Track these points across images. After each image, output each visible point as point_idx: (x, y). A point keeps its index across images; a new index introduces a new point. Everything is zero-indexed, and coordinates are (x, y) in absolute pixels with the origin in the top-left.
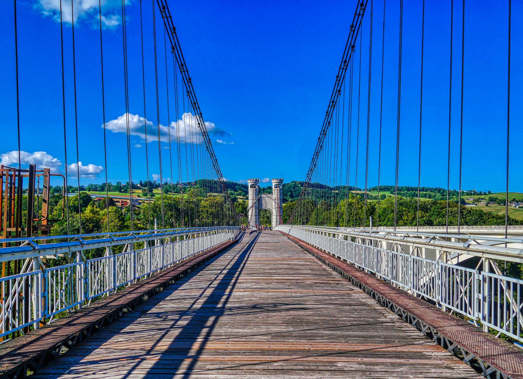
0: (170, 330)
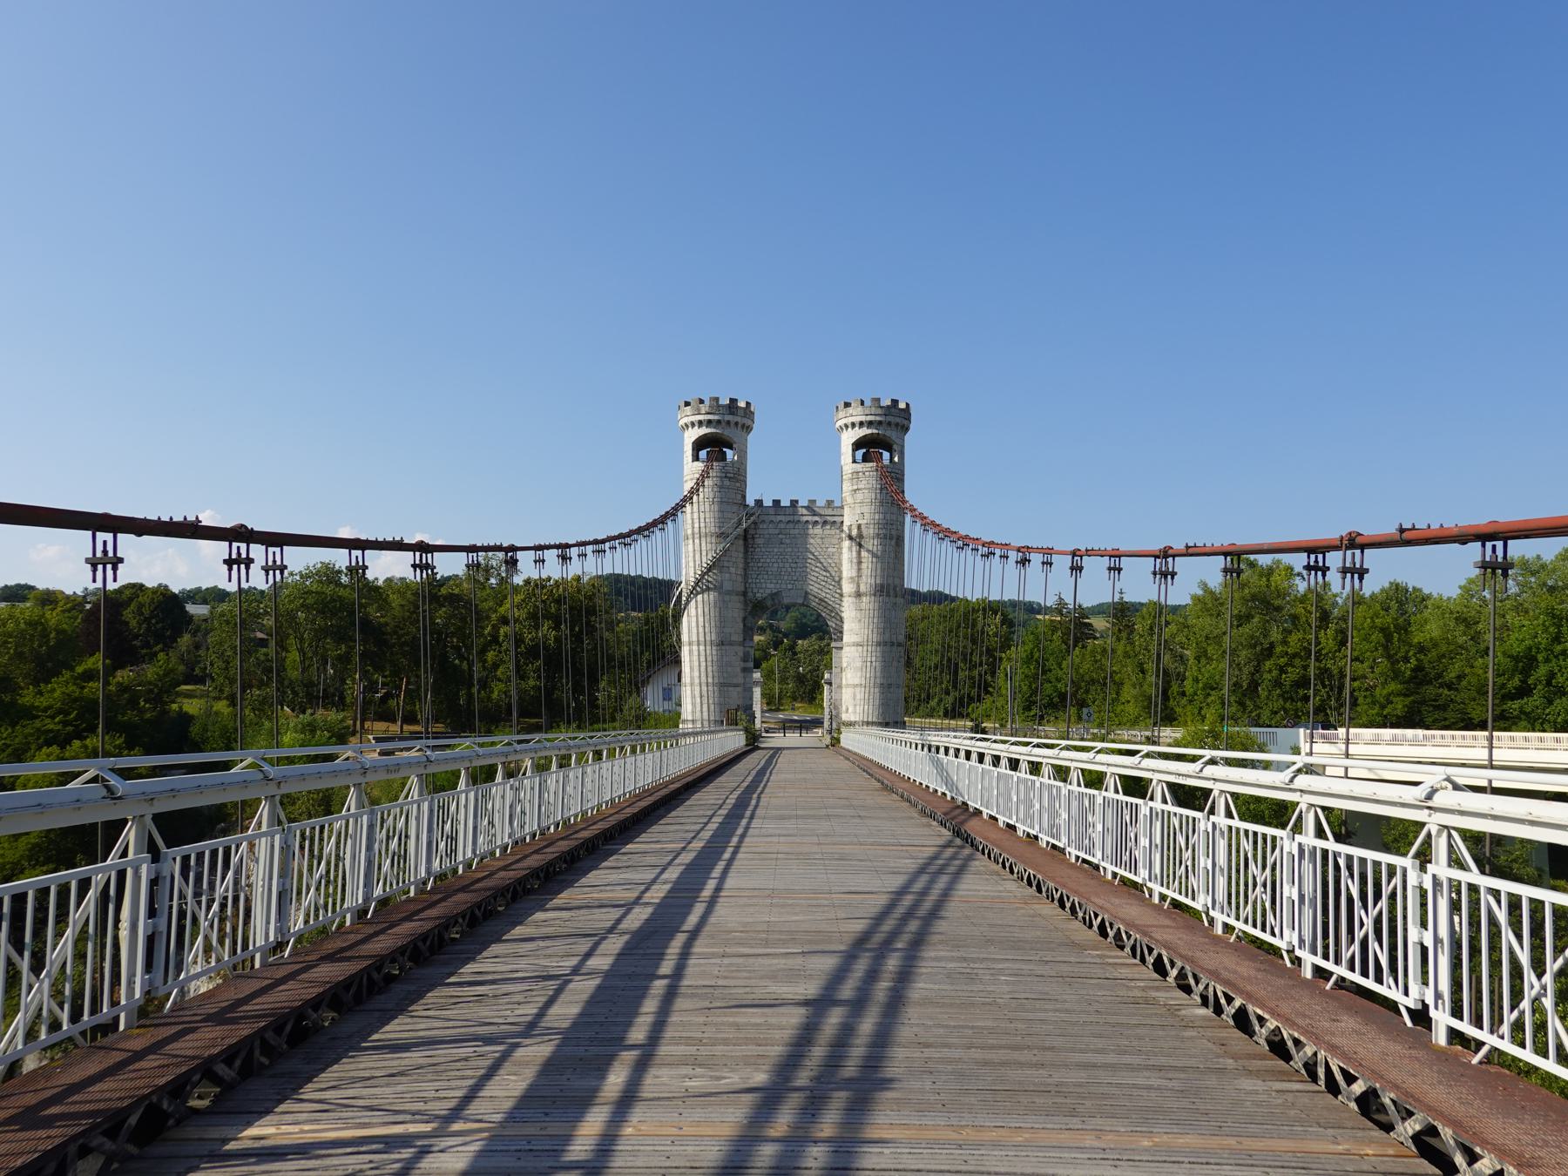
0: (517, 1045)
